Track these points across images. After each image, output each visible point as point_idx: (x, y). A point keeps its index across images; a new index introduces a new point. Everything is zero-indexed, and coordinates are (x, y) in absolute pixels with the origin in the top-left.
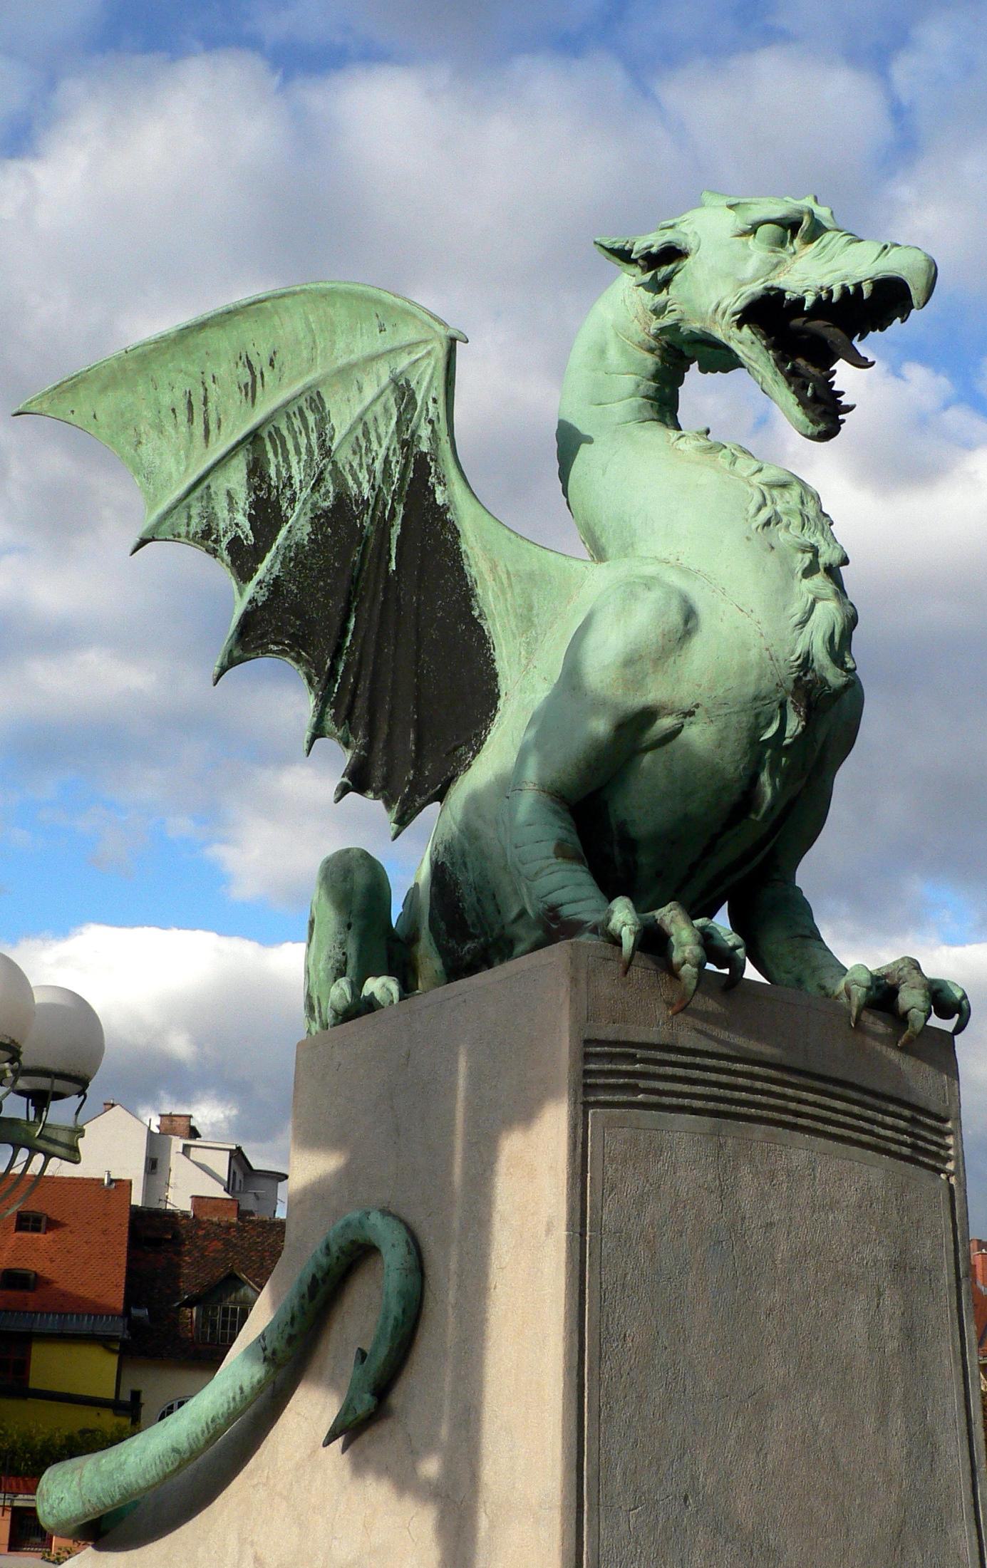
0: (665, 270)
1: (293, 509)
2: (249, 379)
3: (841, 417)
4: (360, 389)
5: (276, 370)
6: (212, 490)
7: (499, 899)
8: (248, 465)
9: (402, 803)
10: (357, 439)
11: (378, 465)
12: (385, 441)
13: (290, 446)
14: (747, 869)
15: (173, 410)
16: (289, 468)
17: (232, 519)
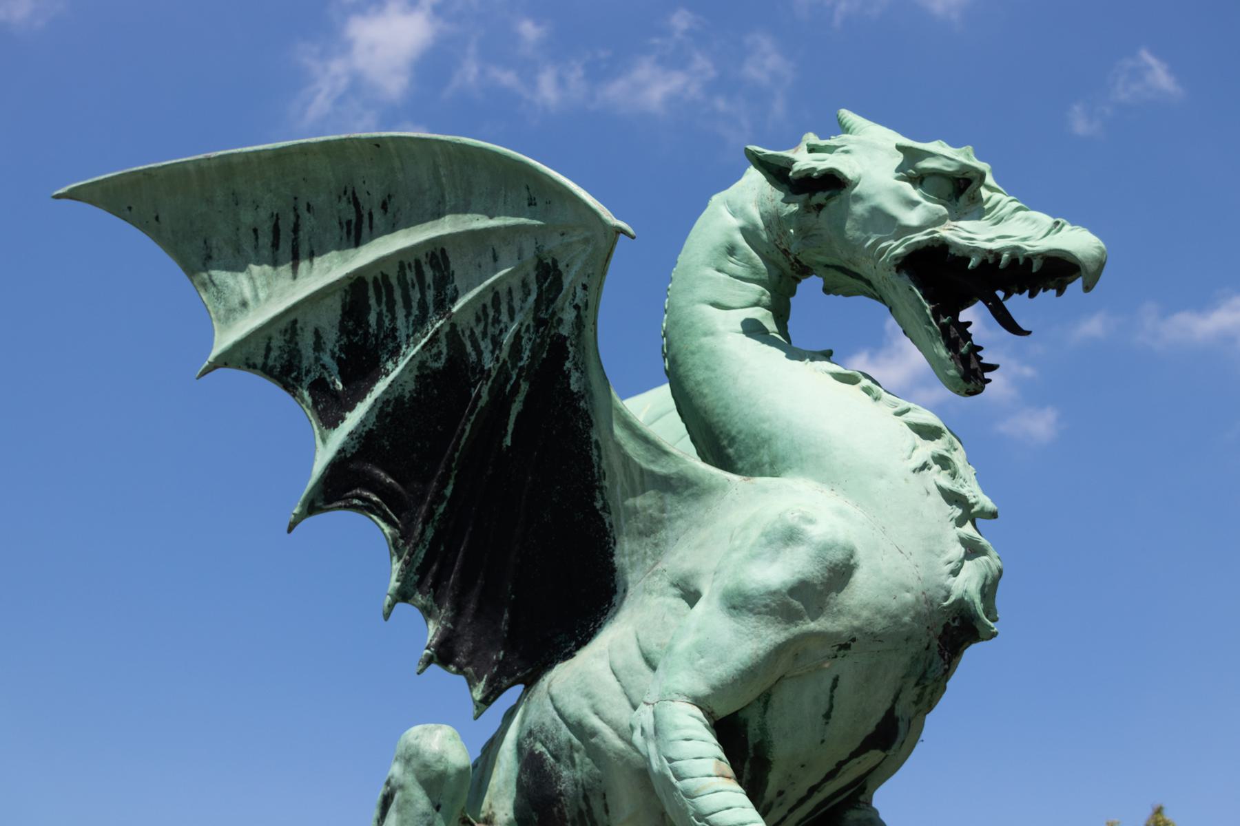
0: (819, 197)
1: (396, 364)
2: (353, 217)
3: (987, 375)
4: (495, 258)
5: (389, 215)
6: (298, 326)
7: (609, 799)
8: (343, 307)
9: (490, 683)
10: (484, 306)
11: (507, 339)
13: (398, 295)
15: (255, 231)
16: (394, 319)
17: (317, 359)
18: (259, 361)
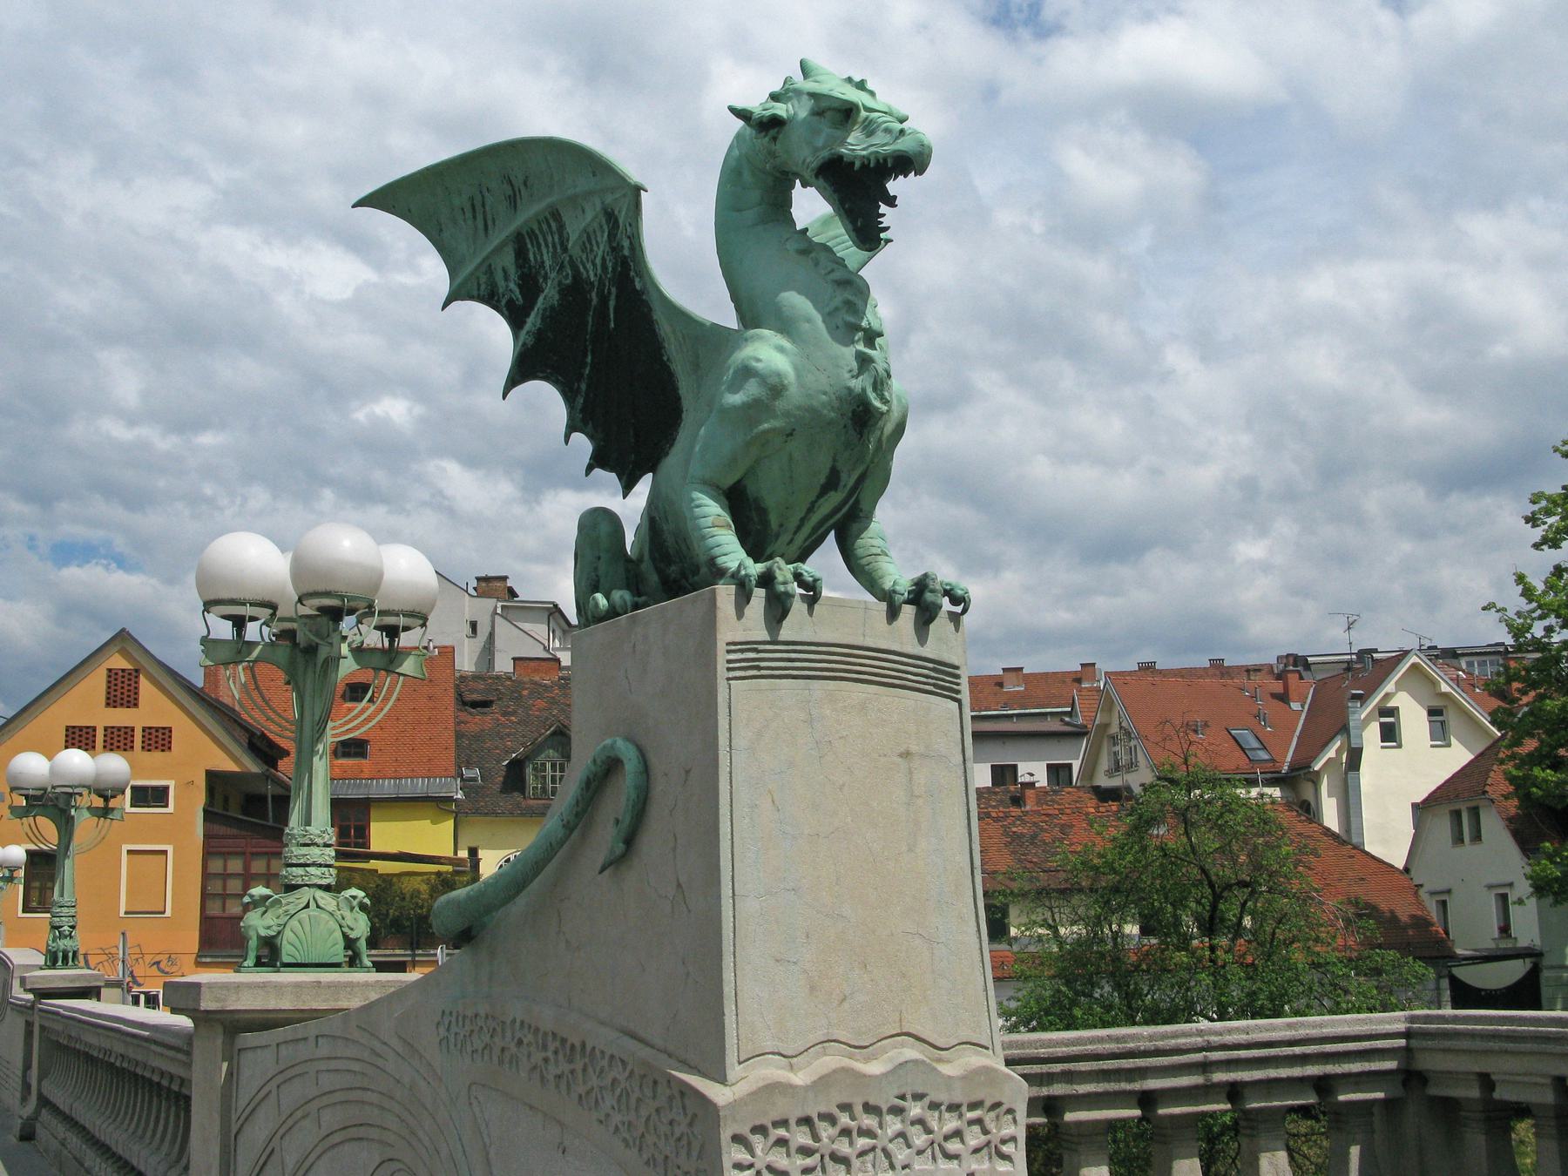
0: (773, 132)
11: (598, 261)
12: (601, 249)
14: (839, 516)
18: (475, 293)
